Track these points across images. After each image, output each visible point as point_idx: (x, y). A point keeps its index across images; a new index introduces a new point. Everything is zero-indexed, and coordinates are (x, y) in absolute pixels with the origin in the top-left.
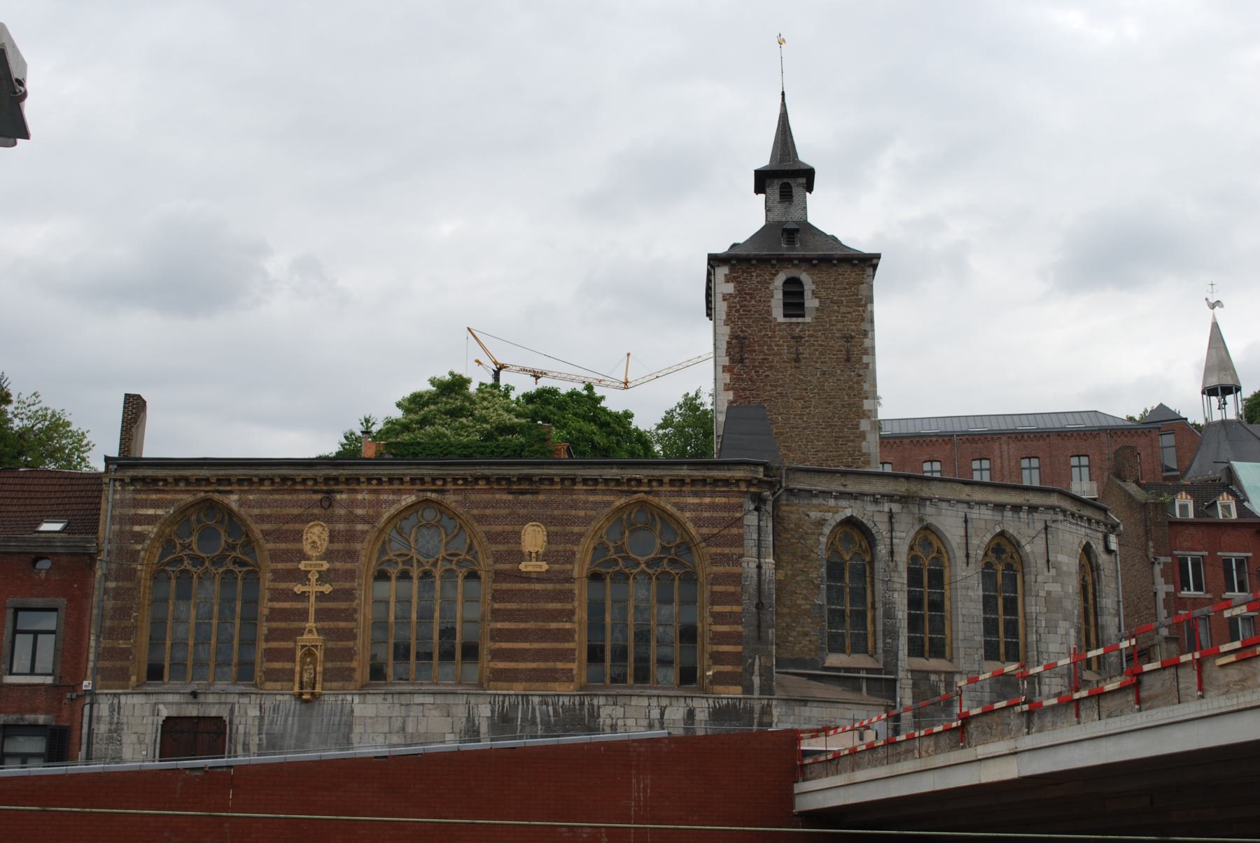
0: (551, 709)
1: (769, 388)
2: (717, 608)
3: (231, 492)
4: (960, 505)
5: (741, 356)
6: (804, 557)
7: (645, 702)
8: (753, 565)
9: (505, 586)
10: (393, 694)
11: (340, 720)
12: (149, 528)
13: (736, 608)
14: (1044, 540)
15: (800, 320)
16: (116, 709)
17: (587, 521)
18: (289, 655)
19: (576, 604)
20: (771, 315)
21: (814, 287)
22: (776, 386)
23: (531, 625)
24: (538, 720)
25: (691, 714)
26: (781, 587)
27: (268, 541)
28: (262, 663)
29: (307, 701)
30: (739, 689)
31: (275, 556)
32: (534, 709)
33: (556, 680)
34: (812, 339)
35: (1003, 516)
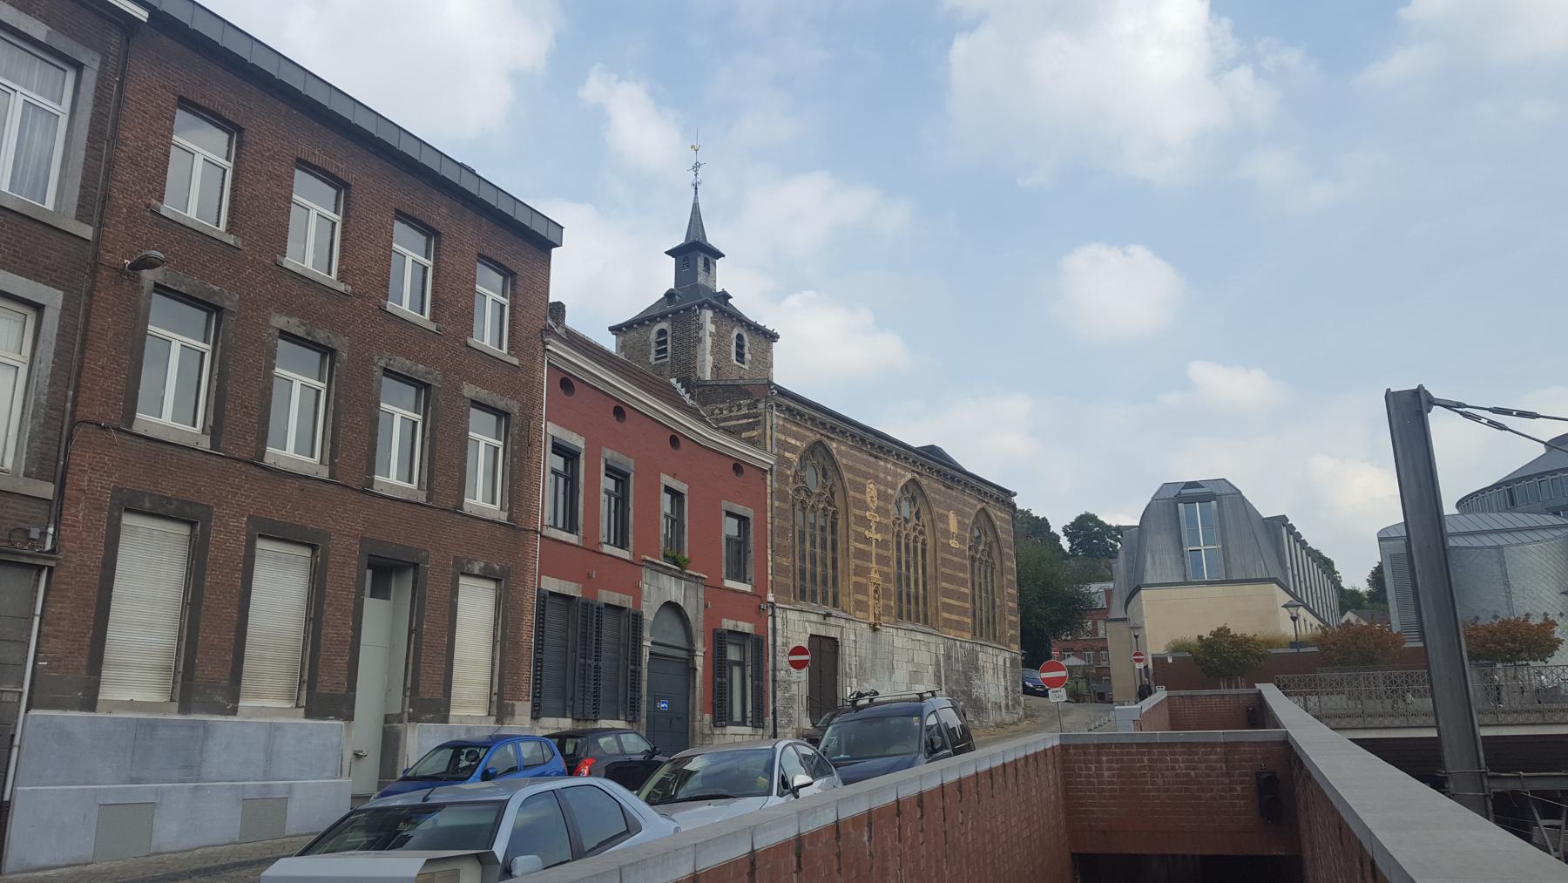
16: (785, 622)
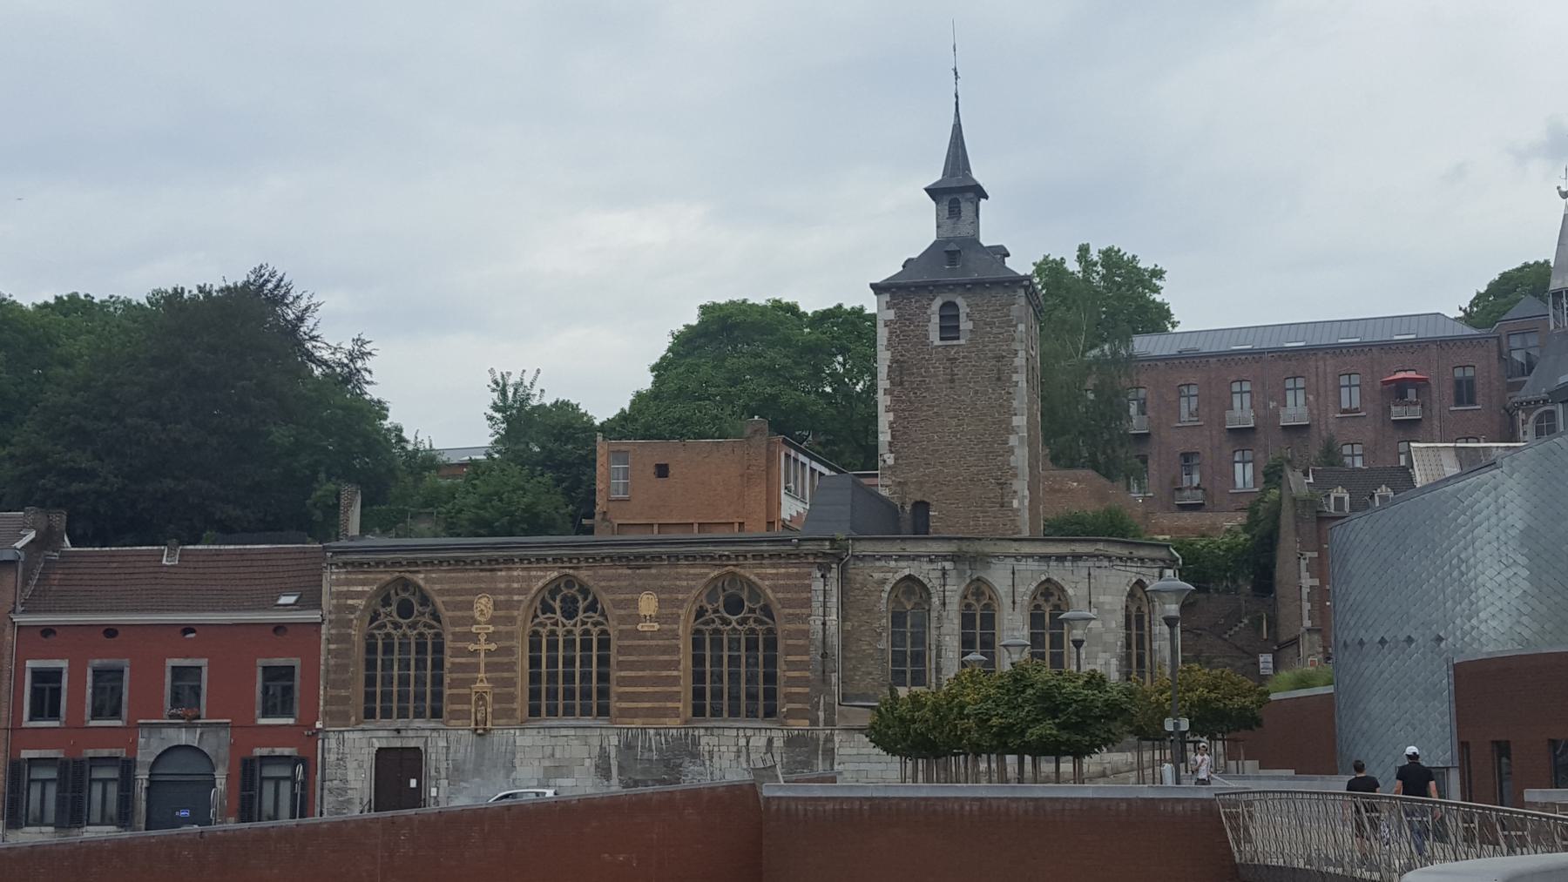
0: (663, 738)
1: (925, 408)
2: (790, 658)
3: (418, 572)
4: (1007, 560)
5: (901, 378)
6: (867, 611)
7: (734, 733)
8: (819, 623)
9: (627, 643)
10: (544, 728)
11: (506, 749)
12: (359, 601)
13: (806, 658)
14: (1087, 584)
15: (955, 342)
17: (689, 589)
18: (465, 699)
19: (681, 656)
20: (928, 339)
21: (968, 310)
22: (933, 407)
23: (646, 673)
24: (654, 747)
25: (770, 741)
26: (847, 638)
27: (447, 610)
28: (447, 705)
29: (480, 735)
30: (807, 722)
31: (454, 622)
32: (650, 739)
33: (665, 716)
34: (966, 360)
35: (1048, 566)
